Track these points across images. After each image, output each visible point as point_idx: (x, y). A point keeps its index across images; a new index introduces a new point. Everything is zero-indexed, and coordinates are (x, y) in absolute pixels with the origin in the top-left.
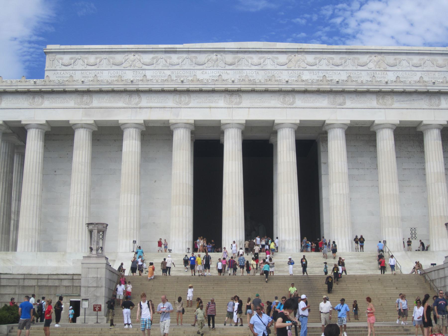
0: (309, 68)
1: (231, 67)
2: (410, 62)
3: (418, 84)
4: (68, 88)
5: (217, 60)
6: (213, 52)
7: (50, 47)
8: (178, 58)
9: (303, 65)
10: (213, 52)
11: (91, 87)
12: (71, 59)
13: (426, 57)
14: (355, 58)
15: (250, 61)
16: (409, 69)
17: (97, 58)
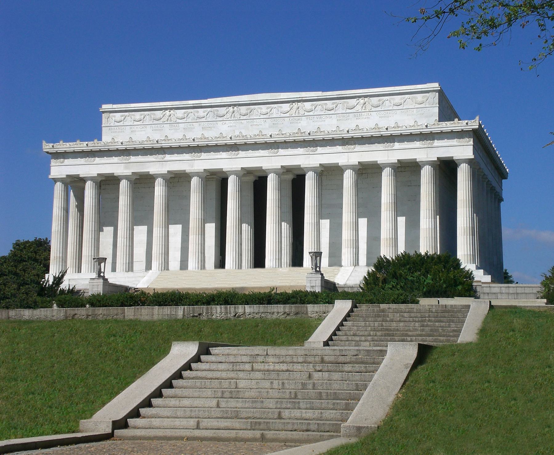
0: (307, 114)
1: (245, 117)
2: (392, 101)
3: (374, 131)
4: (112, 148)
5: (234, 112)
6: (230, 106)
7: (105, 107)
8: (204, 112)
9: (302, 112)
10: (230, 106)
11: (128, 146)
12: (122, 116)
13: (407, 96)
14: (345, 102)
15: (259, 110)
16: (391, 108)
17: (141, 115)
